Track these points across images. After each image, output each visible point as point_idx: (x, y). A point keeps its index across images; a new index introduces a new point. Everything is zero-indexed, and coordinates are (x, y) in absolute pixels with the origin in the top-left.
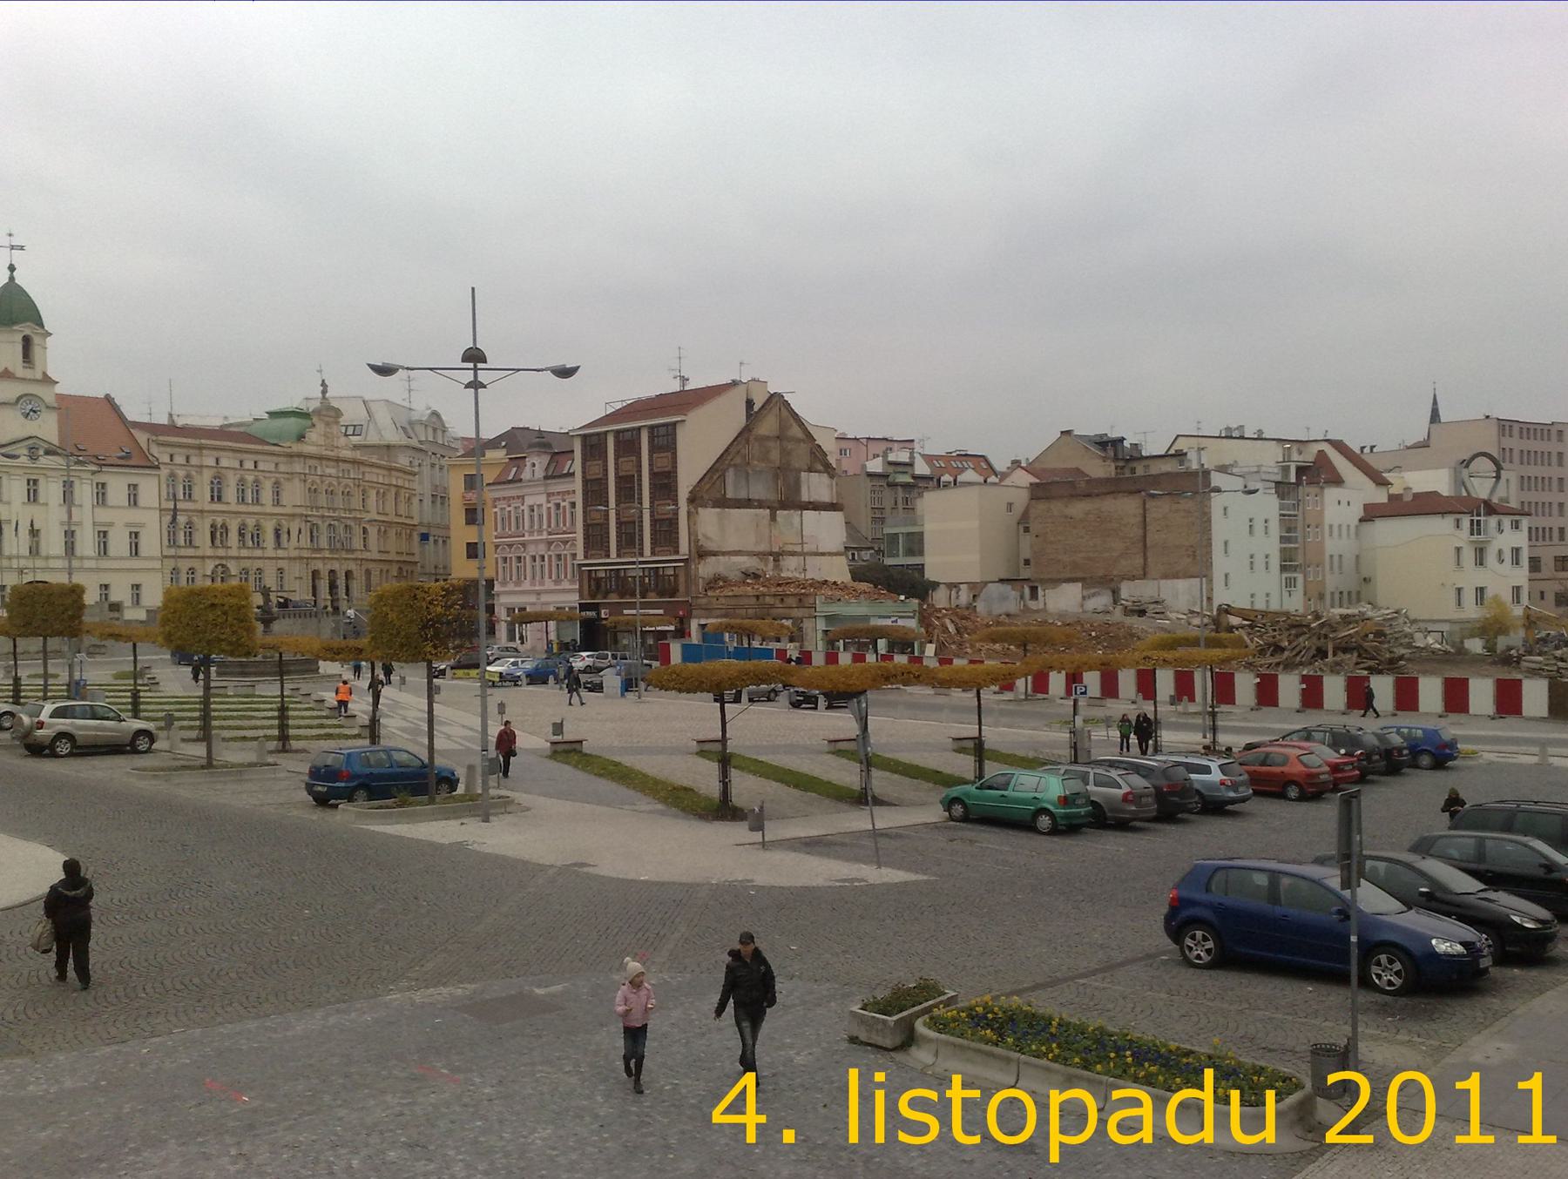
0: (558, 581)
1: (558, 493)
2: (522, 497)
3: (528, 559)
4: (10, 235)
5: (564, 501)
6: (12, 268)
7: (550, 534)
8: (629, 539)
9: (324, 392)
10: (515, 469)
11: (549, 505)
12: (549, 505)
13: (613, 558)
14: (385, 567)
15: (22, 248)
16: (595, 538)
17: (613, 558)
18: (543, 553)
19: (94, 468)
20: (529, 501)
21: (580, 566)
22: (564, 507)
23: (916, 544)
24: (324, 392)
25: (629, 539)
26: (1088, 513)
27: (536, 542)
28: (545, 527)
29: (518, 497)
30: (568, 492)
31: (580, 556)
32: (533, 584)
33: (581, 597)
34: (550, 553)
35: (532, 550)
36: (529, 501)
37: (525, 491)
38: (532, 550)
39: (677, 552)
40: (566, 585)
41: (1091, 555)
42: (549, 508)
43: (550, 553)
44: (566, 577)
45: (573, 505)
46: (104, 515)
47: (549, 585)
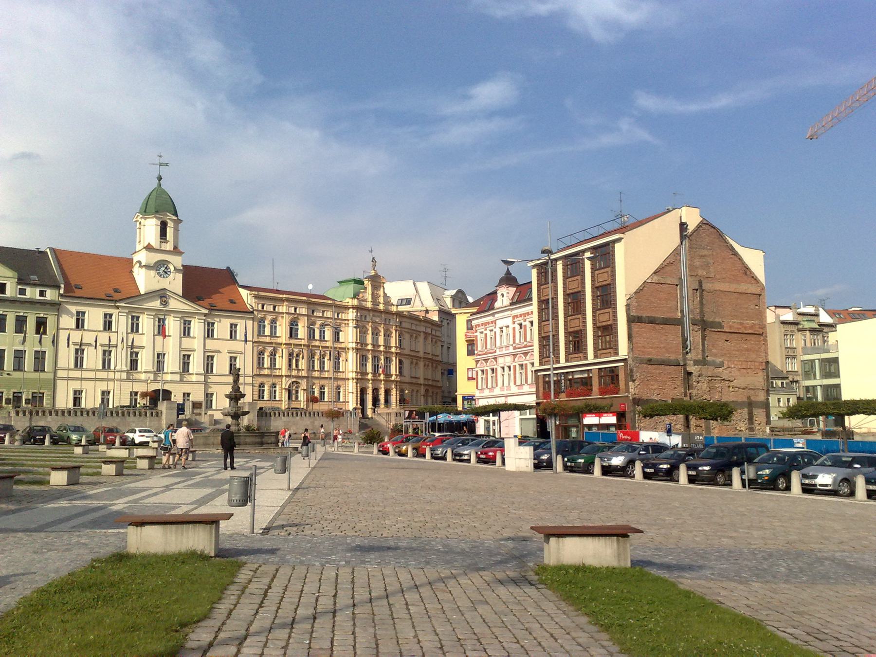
1: (521, 316)
2: (494, 322)
3: (500, 371)
4: (160, 156)
6: (160, 178)
8: (576, 343)
9: (374, 266)
11: (514, 326)
12: (514, 326)
13: (563, 362)
14: (415, 388)
15: (167, 165)
16: (547, 343)
17: (563, 362)
18: (509, 364)
19: (206, 311)
20: (500, 323)
21: (536, 371)
22: (525, 326)
23: (831, 367)
24: (374, 266)
25: (576, 343)
29: (492, 322)
30: (528, 314)
31: (537, 366)
32: (502, 389)
33: (538, 397)
34: (514, 364)
36: (500, 323)
38: (501, 361)
39: (617, 354)
40: (526, 388)
42: (514, 329)
43: (514, 364)
44: (526, 382)
45: (532, 323)
46: (211, 344)
47: (514, 389)
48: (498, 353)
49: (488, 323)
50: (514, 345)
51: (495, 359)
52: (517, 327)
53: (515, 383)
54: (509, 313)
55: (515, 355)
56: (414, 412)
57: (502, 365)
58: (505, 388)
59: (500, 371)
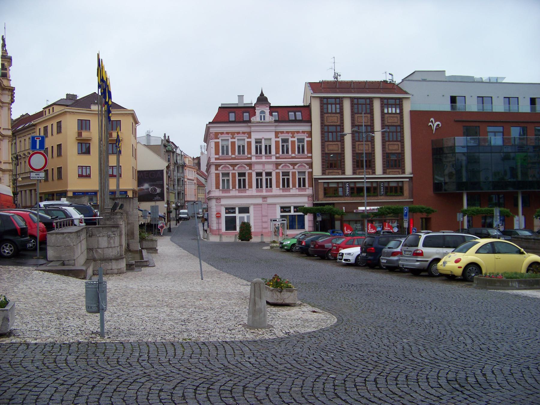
2: (249, 135)
5: (293, 137)
7: (277, 158)
11: (277, 139)
12: (277, 139)
27: (263, 163)
34: (277, 171)
35: (258, 168)
36: (255, 136)
37: (253, 129)
42: (277, 143)
43: (277, 171)
47: (275, 191)
50: (278, 155)
51: (250, 165)
53: (278, 186)
54: (273, 128)
55: (277, 165)
58: (264, 191)
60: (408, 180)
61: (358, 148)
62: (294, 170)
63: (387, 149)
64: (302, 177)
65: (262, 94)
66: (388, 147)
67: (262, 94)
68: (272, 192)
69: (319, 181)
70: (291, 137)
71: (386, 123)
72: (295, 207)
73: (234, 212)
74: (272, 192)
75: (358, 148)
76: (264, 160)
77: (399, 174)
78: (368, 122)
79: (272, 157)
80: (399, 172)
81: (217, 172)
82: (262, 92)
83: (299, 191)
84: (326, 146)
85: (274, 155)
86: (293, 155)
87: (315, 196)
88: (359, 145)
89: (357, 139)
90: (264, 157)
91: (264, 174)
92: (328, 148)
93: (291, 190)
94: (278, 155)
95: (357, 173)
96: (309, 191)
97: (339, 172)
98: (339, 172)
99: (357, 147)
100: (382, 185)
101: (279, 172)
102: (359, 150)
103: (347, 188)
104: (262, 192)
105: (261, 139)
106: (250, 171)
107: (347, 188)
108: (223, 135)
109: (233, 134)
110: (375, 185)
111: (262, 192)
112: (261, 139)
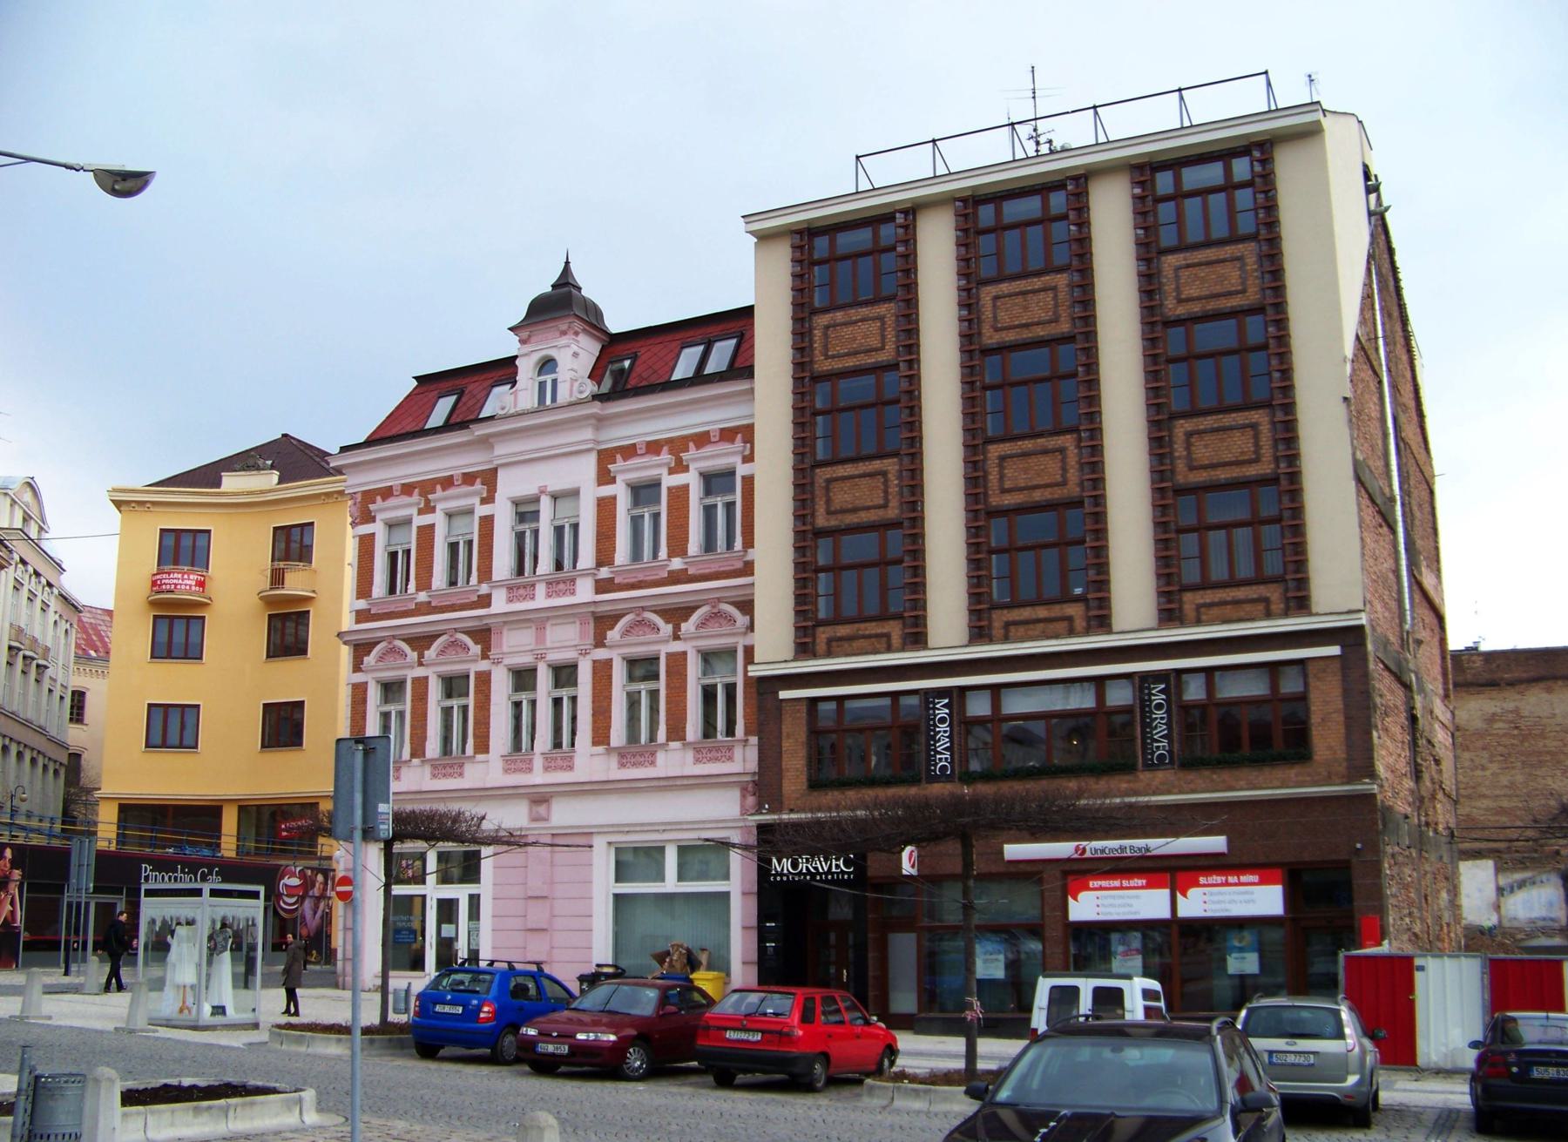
0: (637, 750)
2: (489, 478)
3: (501, 685)
5: (680, 467)
10: (452, 399)
11: (607, 491)
12: (607, 491)
22: (679, 496)
26: (1492, 719)
27: (539, 621)
28: (587, 557)
34: (601, 654)
35: (515, 646)
36: (511, 485)
37: (502, 450)
41: (1505, 804)
42: (606, 507)
43: (601, 654)
47: (589, 762)
48: (500, 604)
49: (448, 482)
50: (604, 573)
51: (483, 635)
52: (620, 492)
53: (601, 736)
54: (587, 434)
55: (603, 622)
56: (8, 853)
57: (525, 660)
58: (538, 762)
59: (501, 685)
60: (1334, 650)
61: (1002, 477)
62: (676, 647)
63: (1181, 465)
64: (719, 681)
65: (566, 282)
66: (1188, 446)
67: (566, 282)
68: (571, 768)
69: (783, 695)
70: (671, 471)
71: (1170, 303)
72: (683, 850)
73: (421, 880)
74: (571, 768)
75: (1002, 477)
76: (541, 600)
77: (1269, 615)
78: (1056, 320)
79: (579, 582)
80: (1266, 601)
81: (359, 678)
82: (567, 263)
83: (697, 761)
84: (819, 492)
85: (585, 573)
86: (677, 564)
87: (764, 787)
88: (1002, 459)
89: (991, 426)
90: (541, 589)
91: (544, 678)
92: (828, 501)
93: (661, 757)
94: (604, 573)
95: (997, 630)
96: (744, 759)
97: (888, 636)
98: (888, 636)
99: (993, 477)
100: (1159, 698)
101: (608, 663)
102: (1004, 491)
103: (943, 727)
104: (530, 770)
105: (536, 500)
106: (483, 665)
107: (943, 727)
108: (392, 502)
109: (425, 488)
110: (1119, 696)
111: (530, 770)
112: (536, 500)
